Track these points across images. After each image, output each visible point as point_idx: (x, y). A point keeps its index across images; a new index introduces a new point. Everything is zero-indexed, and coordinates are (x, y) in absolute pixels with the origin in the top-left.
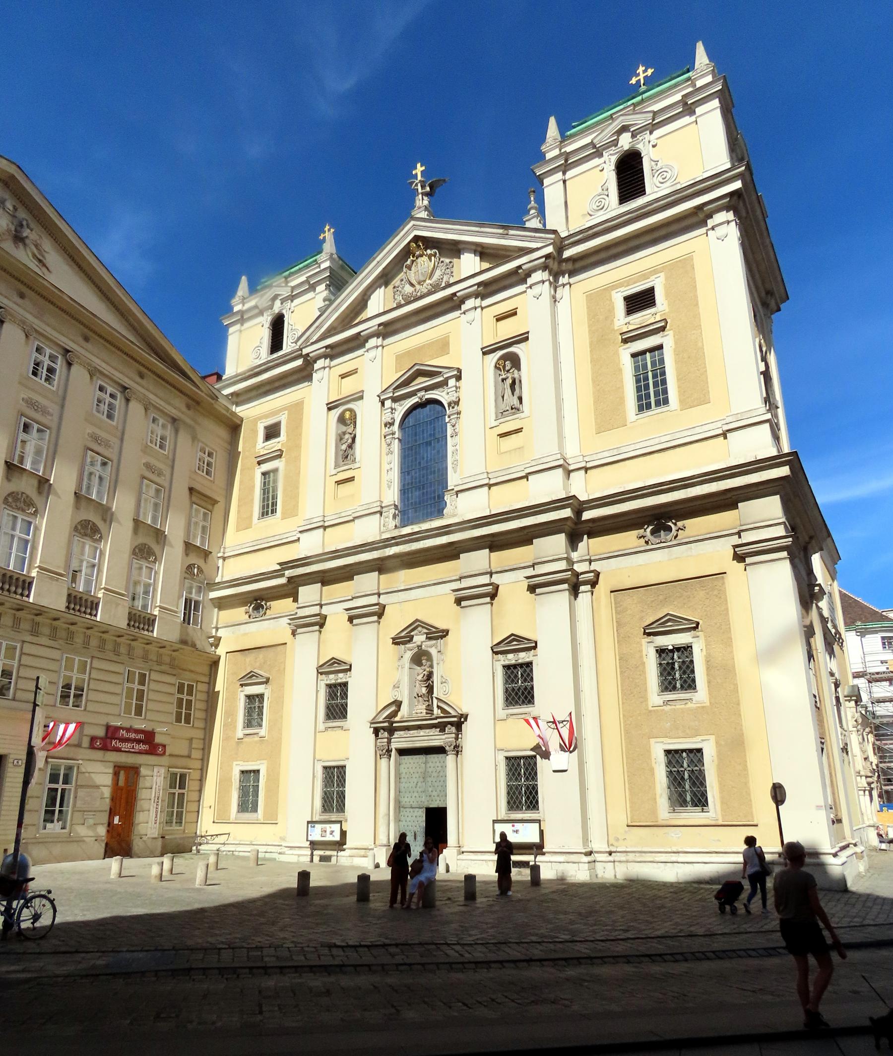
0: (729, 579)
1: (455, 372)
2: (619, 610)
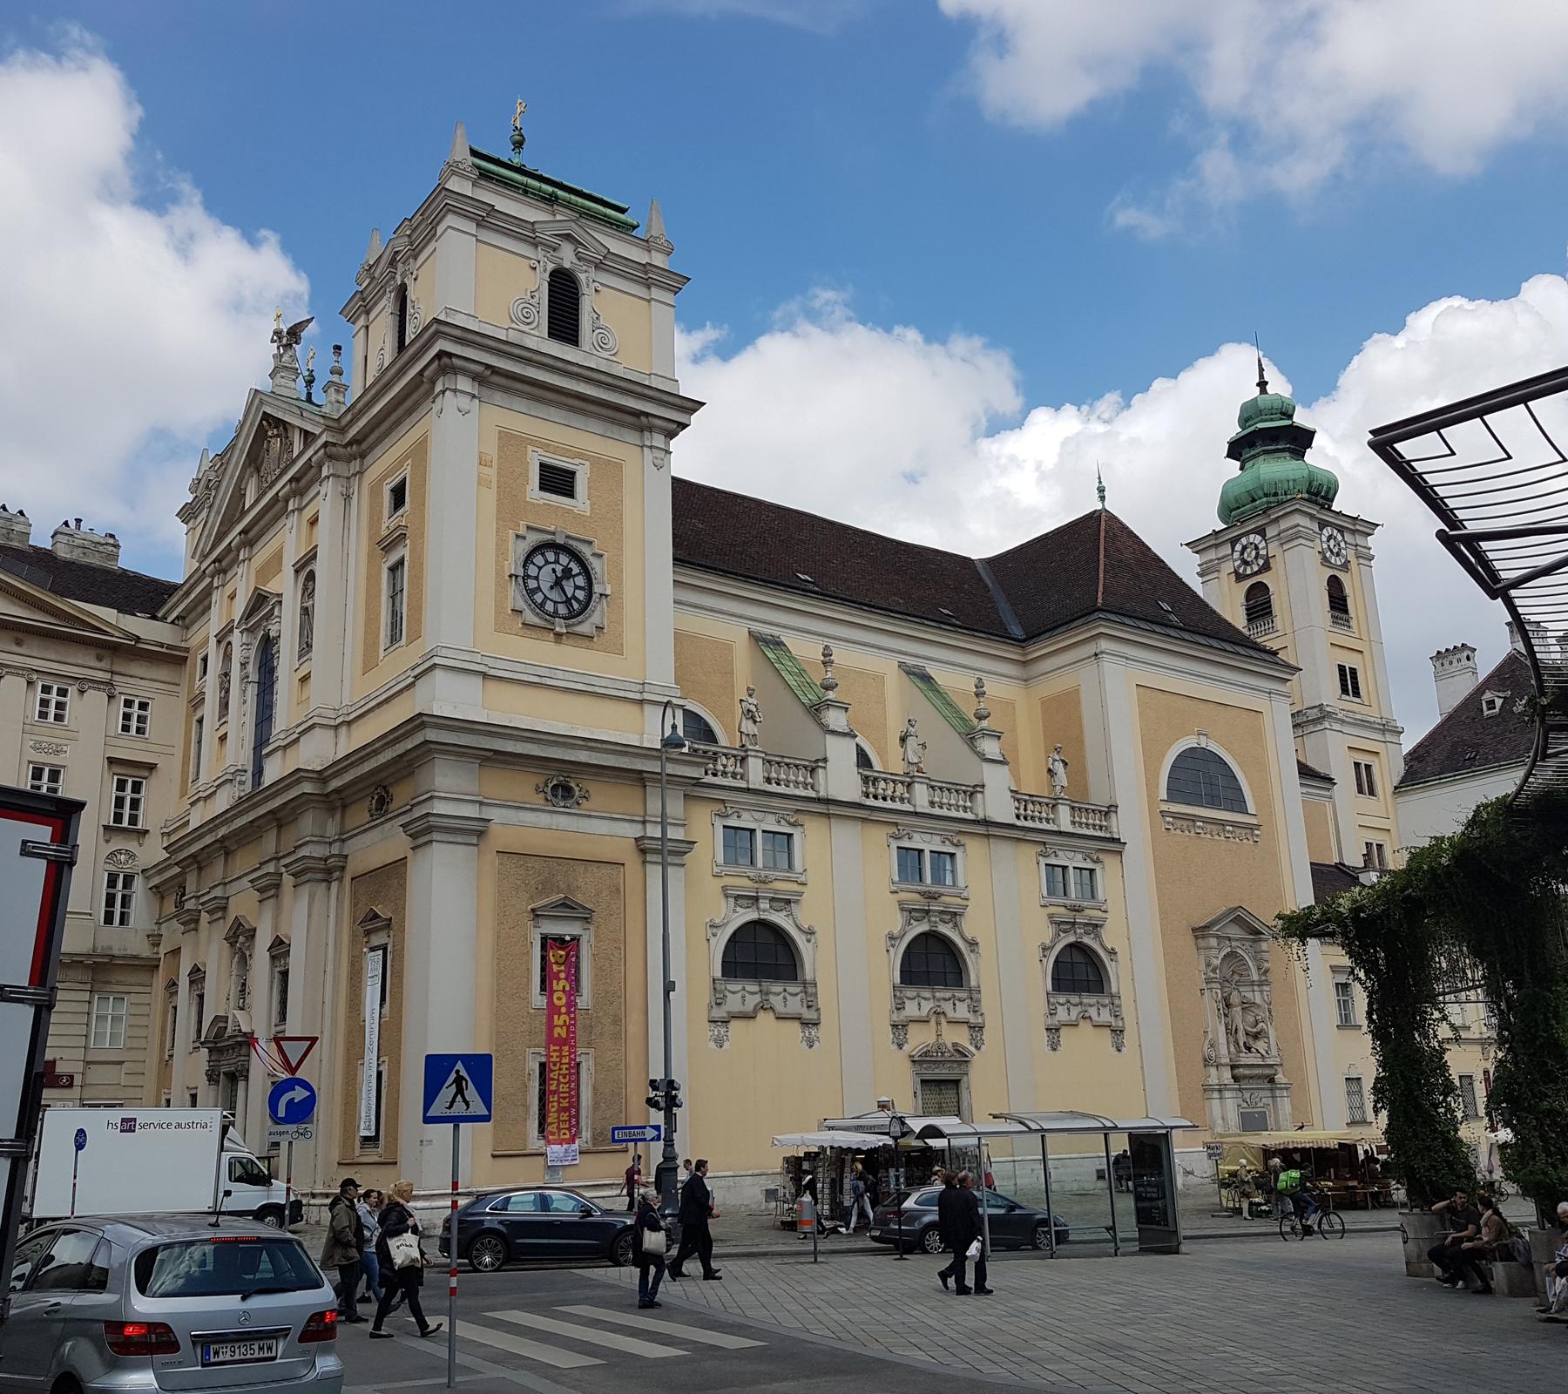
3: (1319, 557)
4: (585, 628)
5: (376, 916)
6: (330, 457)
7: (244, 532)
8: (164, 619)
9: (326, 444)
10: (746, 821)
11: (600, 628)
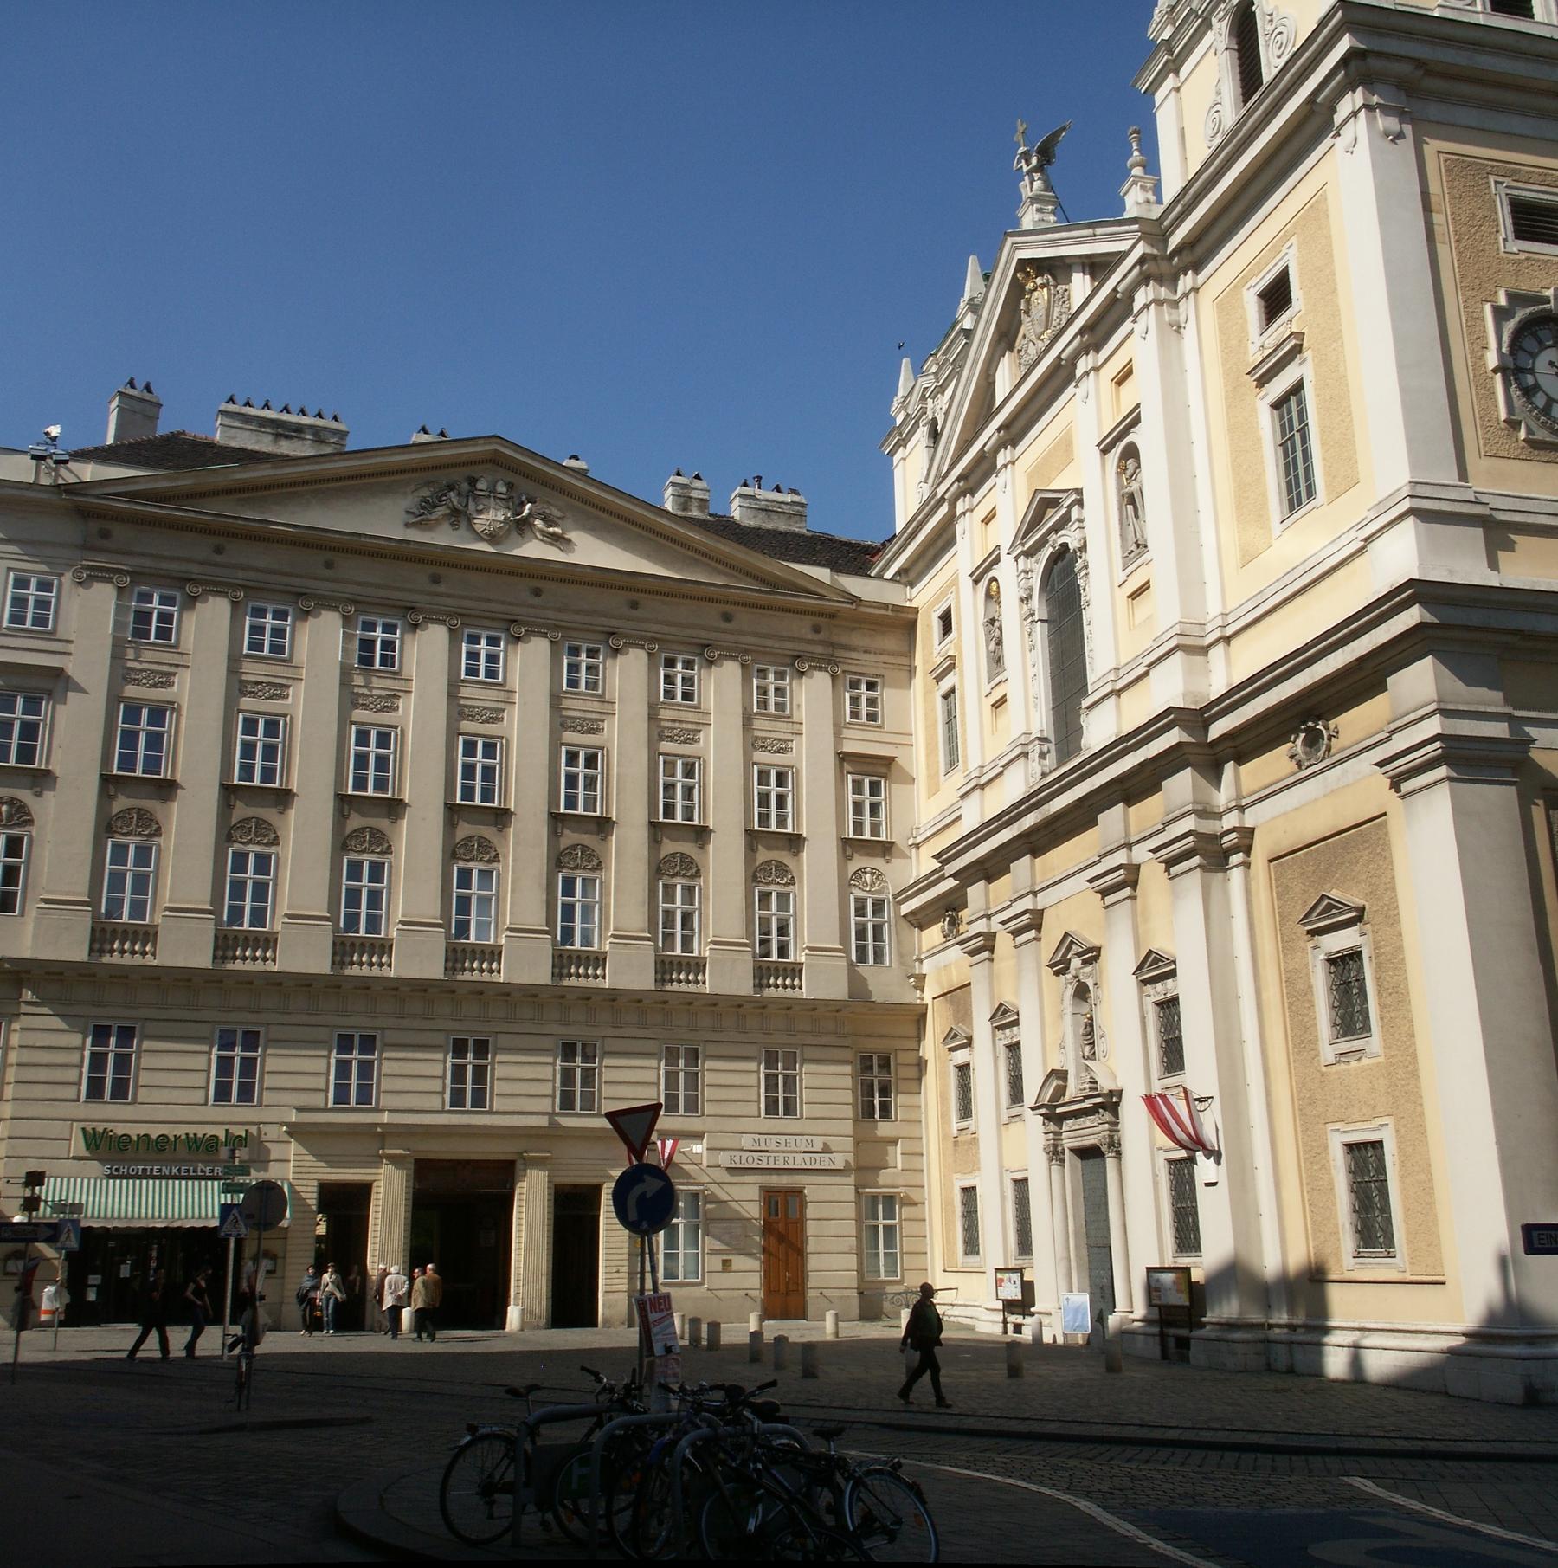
0: (1395, 823)
1: (1074, 497)
2: (1281, 891)
5: (1333, 906)
6: (1144, 279)
7: (1004, 427)
8: (879, 577)
9: (1142, 261)
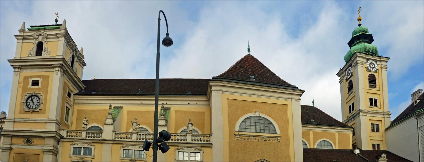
3: (366, 69)
4: (38, 110)
10: (79, 145)
11: (40, 110)
